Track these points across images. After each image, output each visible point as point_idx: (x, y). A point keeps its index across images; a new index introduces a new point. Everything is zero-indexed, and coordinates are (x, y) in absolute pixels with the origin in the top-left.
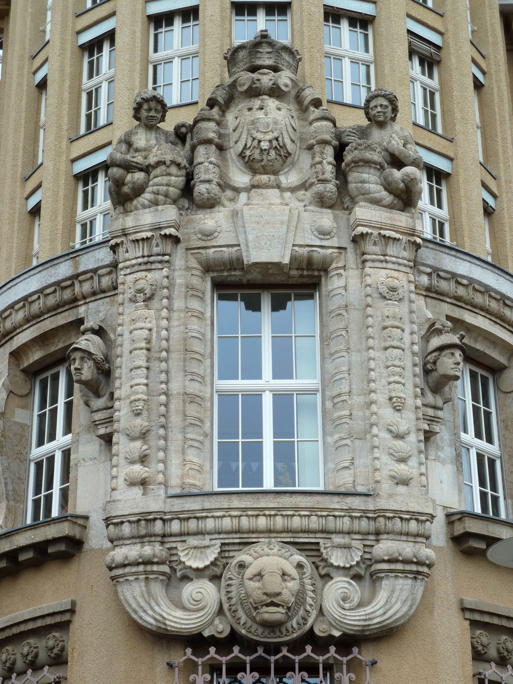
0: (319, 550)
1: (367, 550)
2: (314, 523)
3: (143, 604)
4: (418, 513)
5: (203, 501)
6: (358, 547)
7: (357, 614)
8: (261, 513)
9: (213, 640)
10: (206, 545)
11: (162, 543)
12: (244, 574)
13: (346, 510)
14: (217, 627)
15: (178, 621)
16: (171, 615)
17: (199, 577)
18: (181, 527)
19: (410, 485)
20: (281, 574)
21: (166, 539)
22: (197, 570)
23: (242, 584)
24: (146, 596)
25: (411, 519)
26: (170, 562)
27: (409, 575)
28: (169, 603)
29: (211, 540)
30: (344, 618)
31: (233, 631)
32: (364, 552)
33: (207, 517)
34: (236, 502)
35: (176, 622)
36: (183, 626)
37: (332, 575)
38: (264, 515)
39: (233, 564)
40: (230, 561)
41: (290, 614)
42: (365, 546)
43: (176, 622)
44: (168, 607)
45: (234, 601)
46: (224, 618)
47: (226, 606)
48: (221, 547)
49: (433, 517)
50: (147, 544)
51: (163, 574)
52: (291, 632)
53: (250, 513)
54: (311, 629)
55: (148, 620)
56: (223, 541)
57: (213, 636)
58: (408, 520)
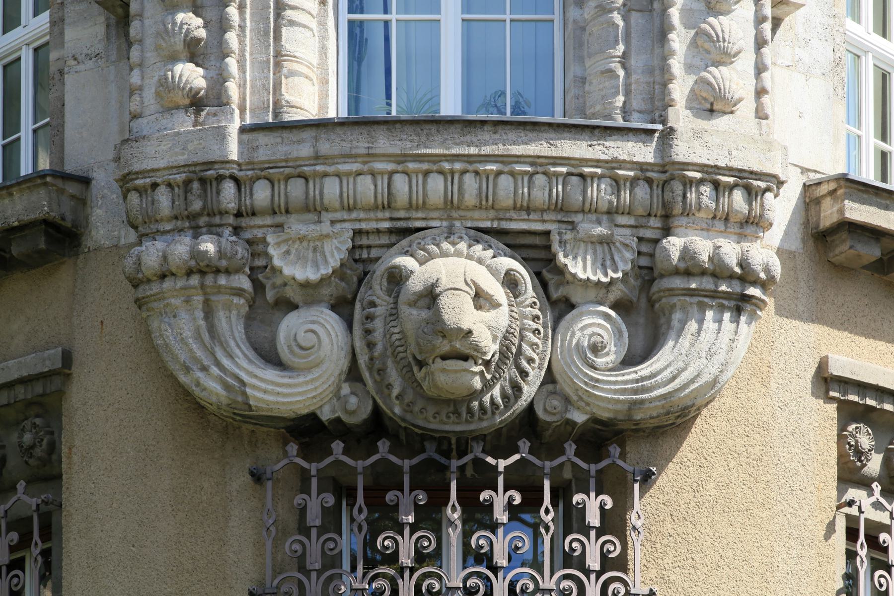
0: (548, 247)
1: (645, 248)
2: (540, 193)
3: (199, 353)
4: (751, 172)
5: (316, 139)
6: (627, 242)
7: (619, 379)
8: (435, 168)
9: (339, 429)
10: (324, 233)
11: (237, 230)
12: (399, 293)
13: (607, 162)
14: (346, 402)
15: (270, 387)
16: (256, 377)
17: (311, 302)
18: (273, 196)
19: (738, 113)
20: (473, 293)
21: (244, 222)
22: (306, 285)
23: (394, 314)
24: (206, 337)
25: (736, 185)
26: (251, 269)
27: (726, 303)
28: (251, 354)
29: (333, 222)
30: (594, 387)
31: (377, 411)
32: (639, 253)
33: (326, 175)
34: (384, 143)
35: (265, 392)
36: (281, 399)
37: (574, 299)
38: (441, 172)
39: (378, 273)
40: (371, 267)
41: (489, 377)
42: (640, 239)
43: (265, 392)
44: (250, 361)
45: (379, 348)
46: (359, 385)
47: (363, 360)
48: (353, 240)
49: (780, 183)
50: (204, 230)
51: (239, 292)
52: (489, 412)
53: (411, 166)
54: (531, 406)
55: (211, 388)
56: (357, 226)
57: (338, 420)
58: (732, 188)
